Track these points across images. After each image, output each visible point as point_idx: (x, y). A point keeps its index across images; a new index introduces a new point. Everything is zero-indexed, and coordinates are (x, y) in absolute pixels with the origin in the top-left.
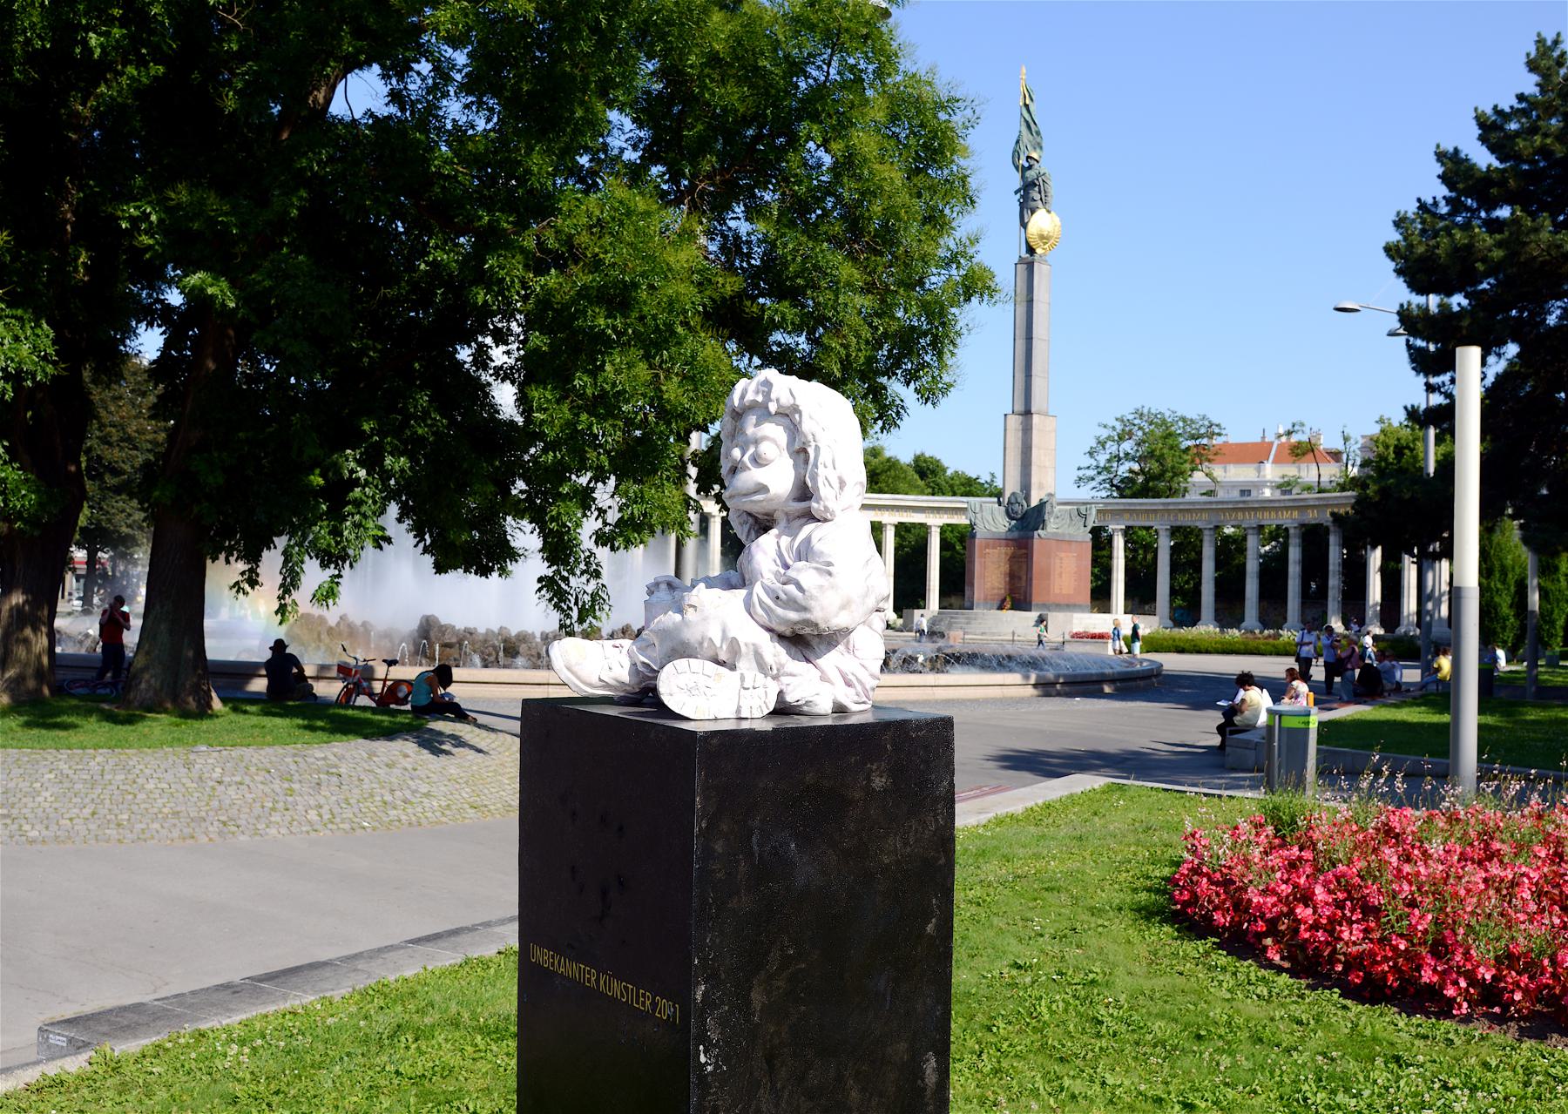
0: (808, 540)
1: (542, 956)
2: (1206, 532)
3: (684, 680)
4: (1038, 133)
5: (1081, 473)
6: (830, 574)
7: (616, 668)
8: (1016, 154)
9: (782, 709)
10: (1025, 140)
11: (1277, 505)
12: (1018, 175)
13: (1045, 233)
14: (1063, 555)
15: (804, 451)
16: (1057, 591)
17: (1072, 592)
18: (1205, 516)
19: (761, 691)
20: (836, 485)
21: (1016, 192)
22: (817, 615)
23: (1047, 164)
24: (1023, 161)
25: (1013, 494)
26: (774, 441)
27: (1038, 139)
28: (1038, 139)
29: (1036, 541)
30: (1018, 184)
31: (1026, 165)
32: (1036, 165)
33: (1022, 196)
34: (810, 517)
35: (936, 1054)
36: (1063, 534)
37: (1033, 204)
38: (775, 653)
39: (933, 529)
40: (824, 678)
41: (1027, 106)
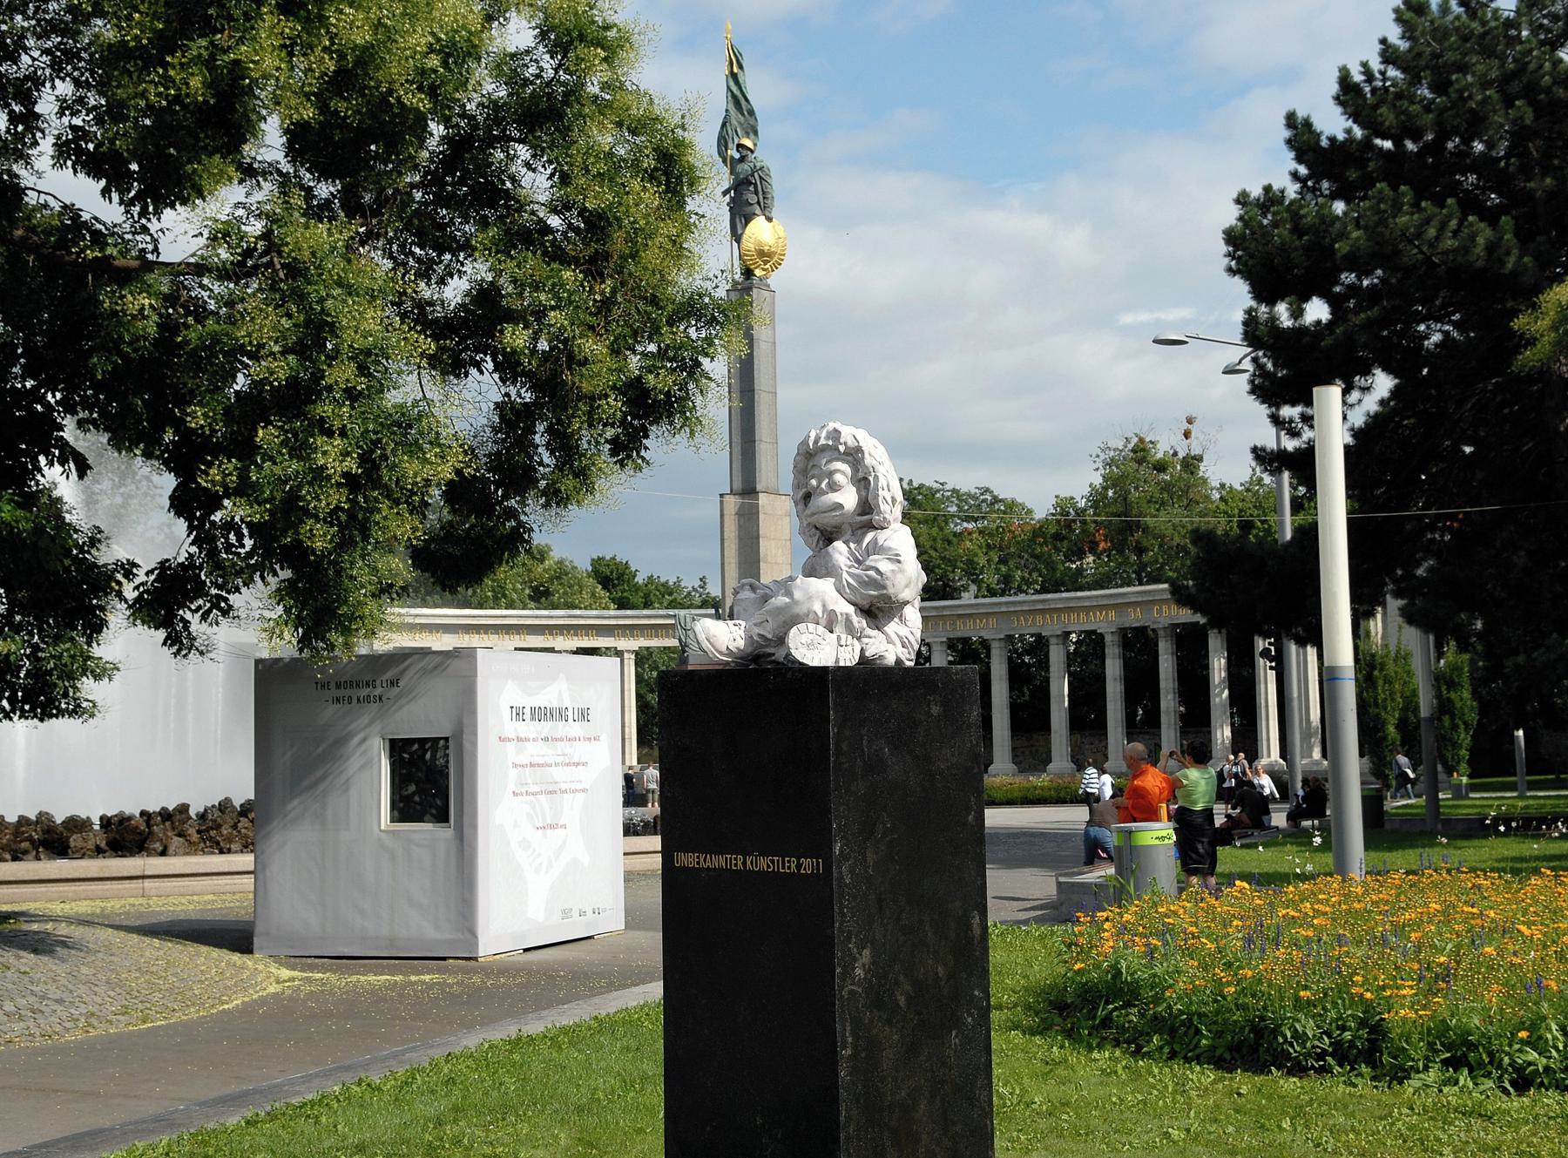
0: (875, 541)
1: (686, 860)
3: (805, 638)
4: (751, 112)
6: (899, 562)
7: (738, 638)
9: (863, 660)
10: (734, 122)
12: (727, 171)
15: (865, 479)
18: (993, 622)
19: (850, 648)
20: (890, 501)
21: (725, 193)
22: (891, 591)
23: (766, 153)
24: (733, 152)
26: (843, 473)
32: (751, 157)
34: (871, 526)
35: (980, 913)
37: (748, 209)
38: (859, 622)
40: (890, 641)
41: (734, 76)
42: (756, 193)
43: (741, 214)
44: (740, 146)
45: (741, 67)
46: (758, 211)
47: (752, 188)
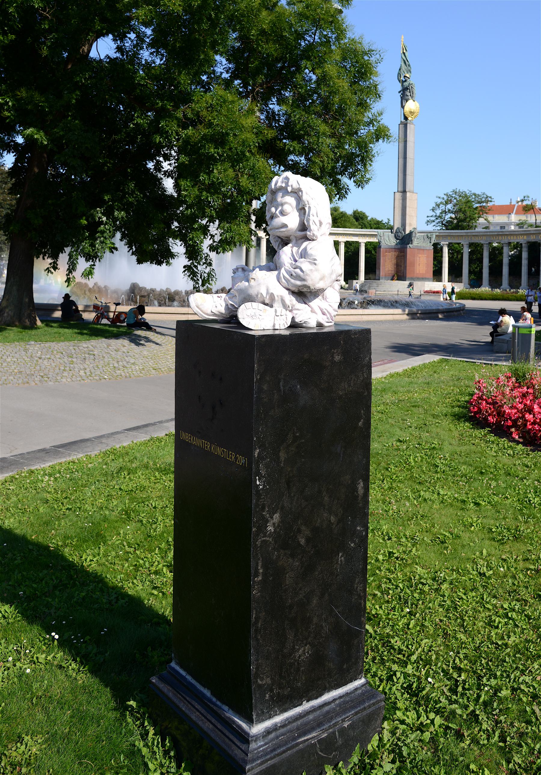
0: (305, 249)
1: (186, 436)
2: (485, 245)
3: (249, 312)
4: (409, 65)
5: (428, 219)
6: (315, 264)
7: (219, 306)
8: (399, 75)
9: (294, 325)
11: (517, 233)
12: (400, 85)
13: (412, 111)
14: (420, 255)
15: (304, 209)
16: (418, 272)
17: (424, 272)
18: (484, 238)
19: (284, 317)
20: (318, 224)
21: (399, 92)
22: (309, 283)
23: (413, 79)
24: (402, 78)
25: (398, 228)
26: (290, 204)
27: (409, 68)
28: (409, 68)
29: (408, 250)
30: (400, 88)
31: (404, 80)
32: (408, 80)
33: (402, 94)
34: (306, 238)
35: (363, 480)
36: (421, 246)
37: (407, 97)
38: (290, 300)
39: (362, 244)
40: (313, 311)
41: (404, 53)
42: (410, 92)
43: (404, 98)
44: (405, 76)
45: (406, 50)
46: (410, 98)
47: (408, 90)
